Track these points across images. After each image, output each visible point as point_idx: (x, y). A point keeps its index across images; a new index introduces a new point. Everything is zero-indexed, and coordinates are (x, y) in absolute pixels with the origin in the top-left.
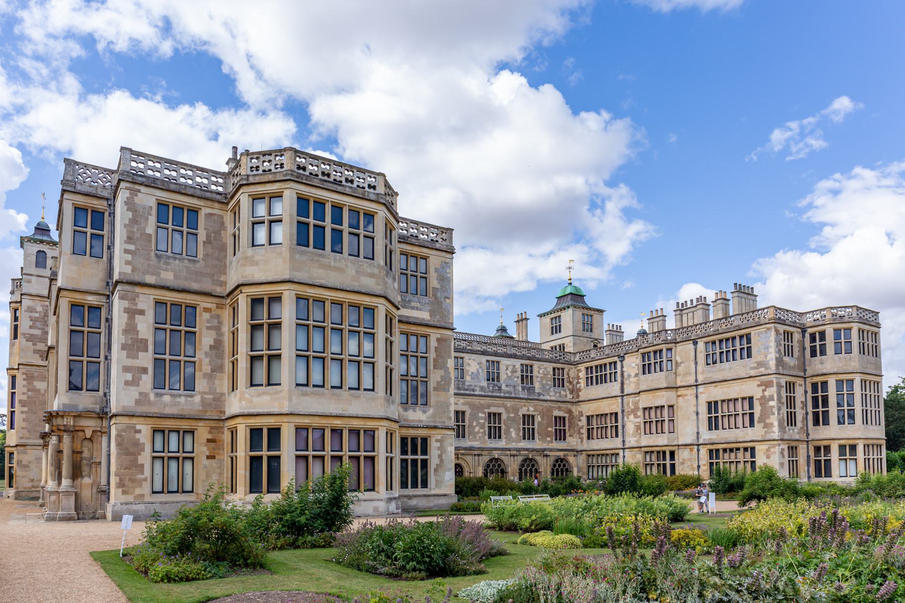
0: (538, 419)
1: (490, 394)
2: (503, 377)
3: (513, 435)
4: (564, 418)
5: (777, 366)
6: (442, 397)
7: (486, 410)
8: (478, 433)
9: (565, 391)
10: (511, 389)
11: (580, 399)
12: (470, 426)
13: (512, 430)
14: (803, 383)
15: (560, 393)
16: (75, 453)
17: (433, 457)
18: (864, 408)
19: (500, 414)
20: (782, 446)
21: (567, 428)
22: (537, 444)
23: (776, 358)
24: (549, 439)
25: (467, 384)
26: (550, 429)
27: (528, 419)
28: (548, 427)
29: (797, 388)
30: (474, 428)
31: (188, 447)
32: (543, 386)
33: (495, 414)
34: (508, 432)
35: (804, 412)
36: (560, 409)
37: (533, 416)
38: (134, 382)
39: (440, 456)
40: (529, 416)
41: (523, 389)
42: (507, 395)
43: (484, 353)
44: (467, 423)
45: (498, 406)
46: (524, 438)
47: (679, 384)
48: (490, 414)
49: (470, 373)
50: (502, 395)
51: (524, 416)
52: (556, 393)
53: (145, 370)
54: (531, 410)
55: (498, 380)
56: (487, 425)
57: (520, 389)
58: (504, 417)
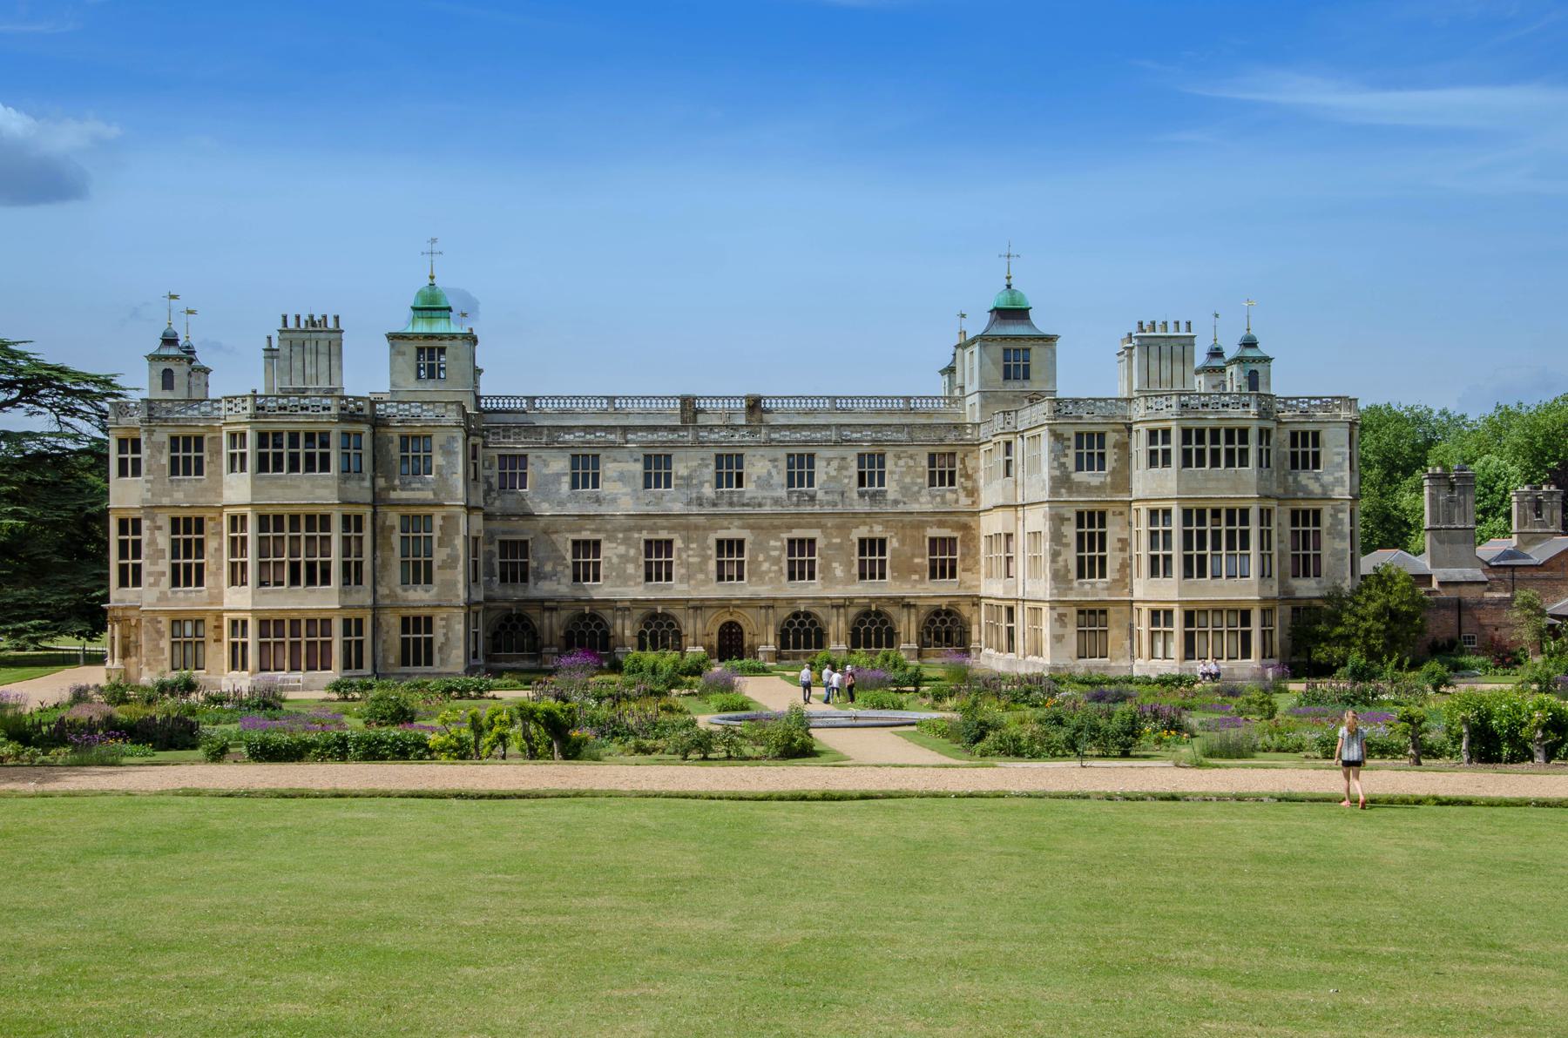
0: (893, 544)
1: (793, 510)
2: (819, 478)
3: (839, 571)
4: (954, 539)
5: (1054, 490)
6: (448, 574)
7: (785, 536)
8: (770, 571)
9: (955, 492)
10: (837, 498)
11: (982, 507)
12: (753, 561)
13: (835, 565)
14: (1124, 509)
15: (943, 497)
16: (124, 637)
17: (438, 636)
18: (1195, 552)
19: (812, 542)
20: (1061, 610)
21: (958, 556)
22: (889, 587)
23: (1053, 478)
24: (915, 577)
25: (747, 495)
26: (917, 560)
27: (872, 546)
28: (914, 556)
29: (1109, 518)
30: (760, 563)
31: (200, 632)
32: (905, 489)
33: (801, 541)
34: (827, 568)
35: (1127, 555)
36: (941, 524)
37: (883, 542)
38: (156, 584)
39: (445, 635)
40: (872, 541)
41: (862, 495)
42: (828, 509)
43: (782, 444)
44: (746, 558)
45: (810, 526)
46: (862, 576)
47: (1020, 501)
48: (791, 542)
49: (754, 478)
50: (817, 509)
51: (862, 541)
52: (933, 497)
53: (163, 574)
54: (878, 531)
55: (811, 484)
56: (785, 558)
57: (856, 496)
58: (818, 545)
